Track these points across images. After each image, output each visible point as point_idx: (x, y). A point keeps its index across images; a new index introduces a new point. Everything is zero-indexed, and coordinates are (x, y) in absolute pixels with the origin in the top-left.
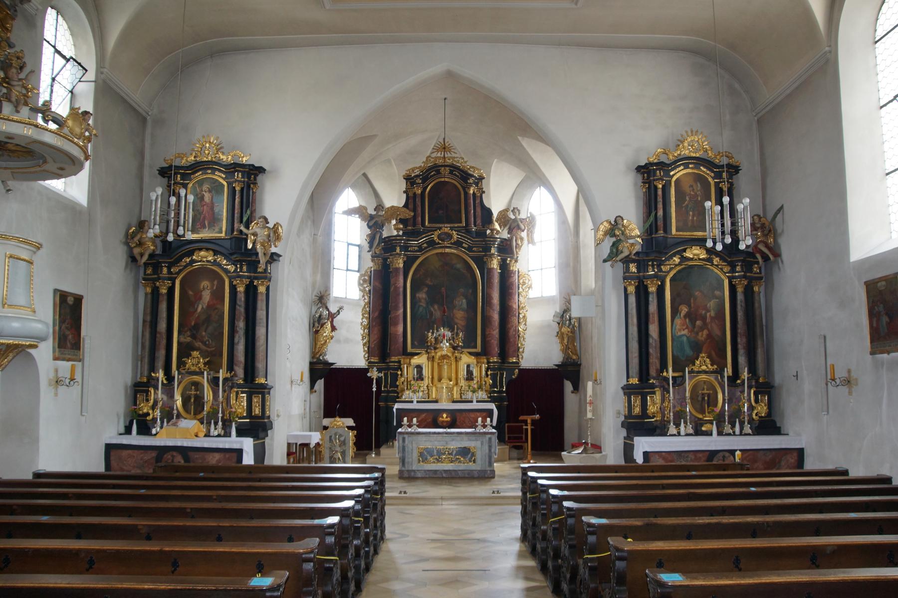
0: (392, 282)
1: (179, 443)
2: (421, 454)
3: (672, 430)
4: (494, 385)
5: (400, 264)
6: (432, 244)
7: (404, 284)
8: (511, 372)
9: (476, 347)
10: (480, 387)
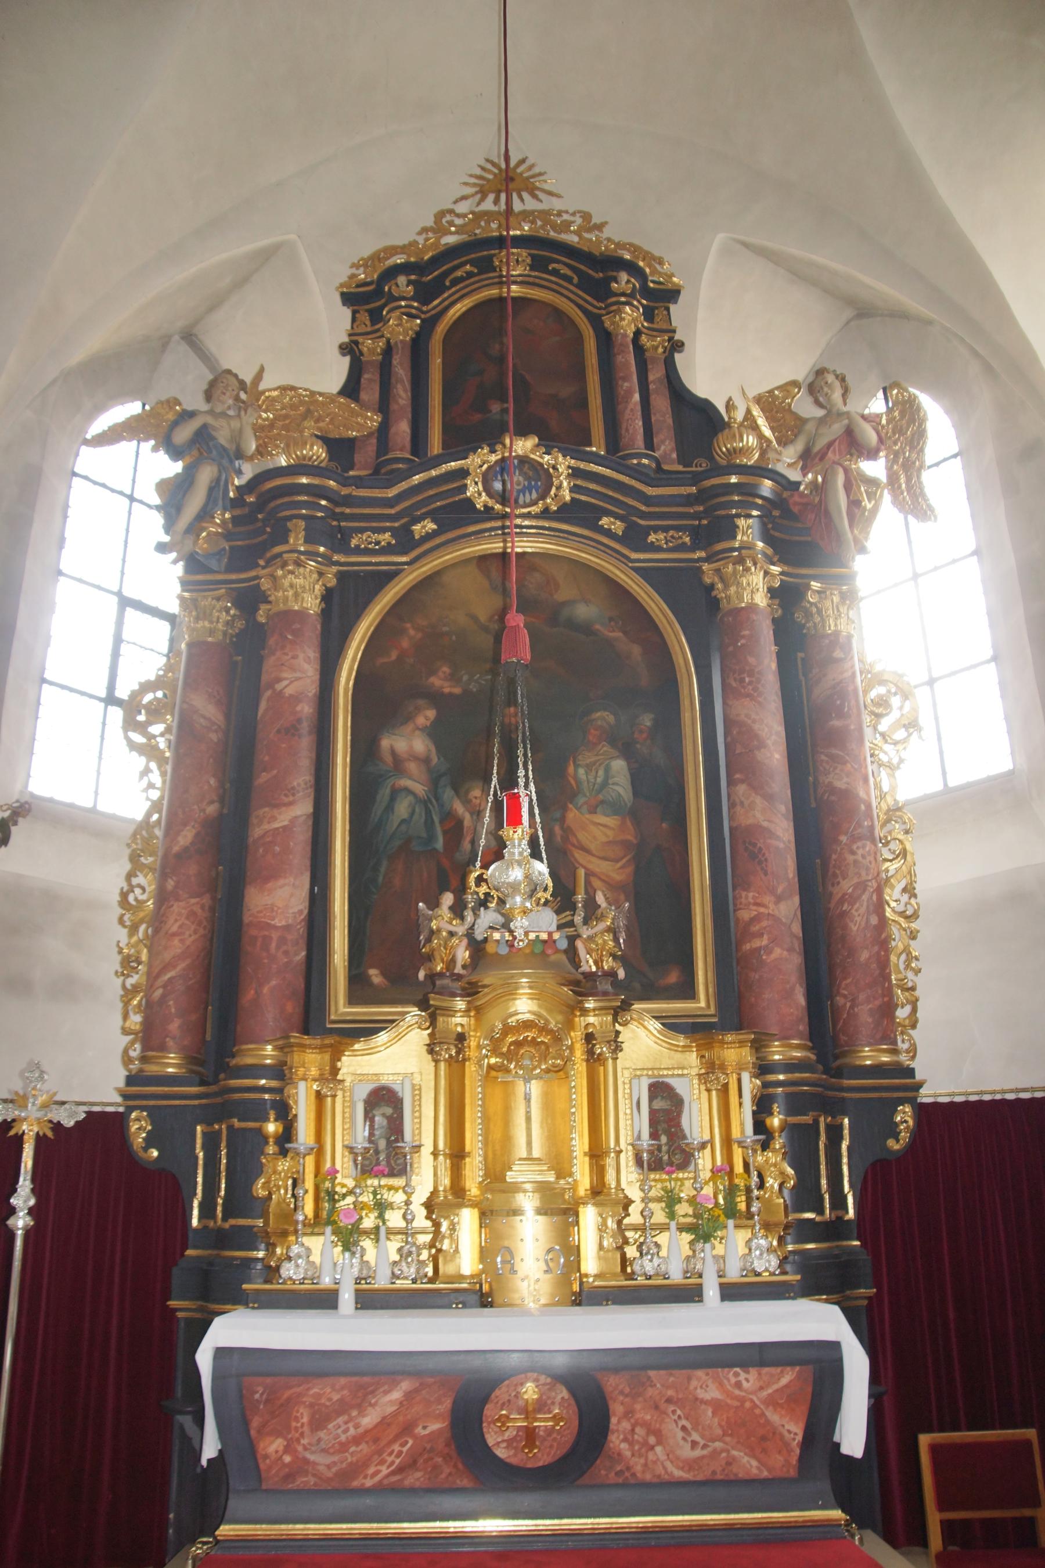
0: (265, 678)
5: (301, 586)
6: (458, 515)
8: (876, 1118)
9: (687, 991)
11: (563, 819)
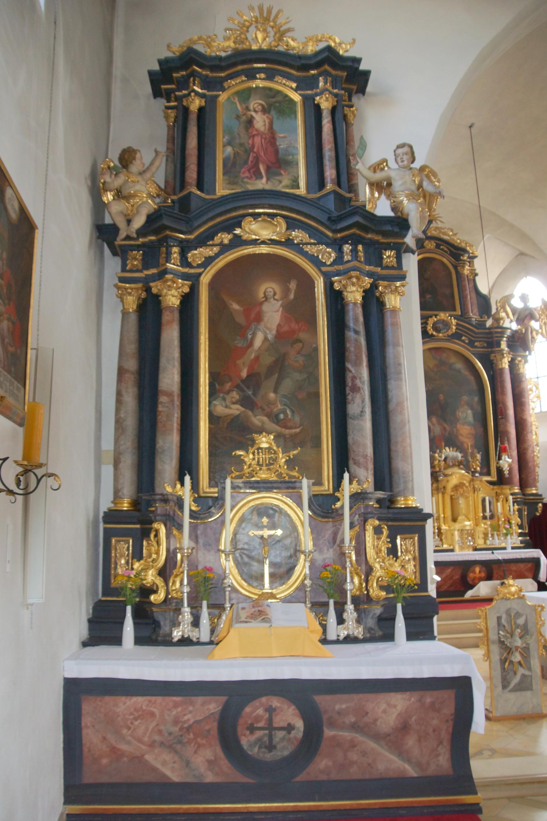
11: (456, 427)
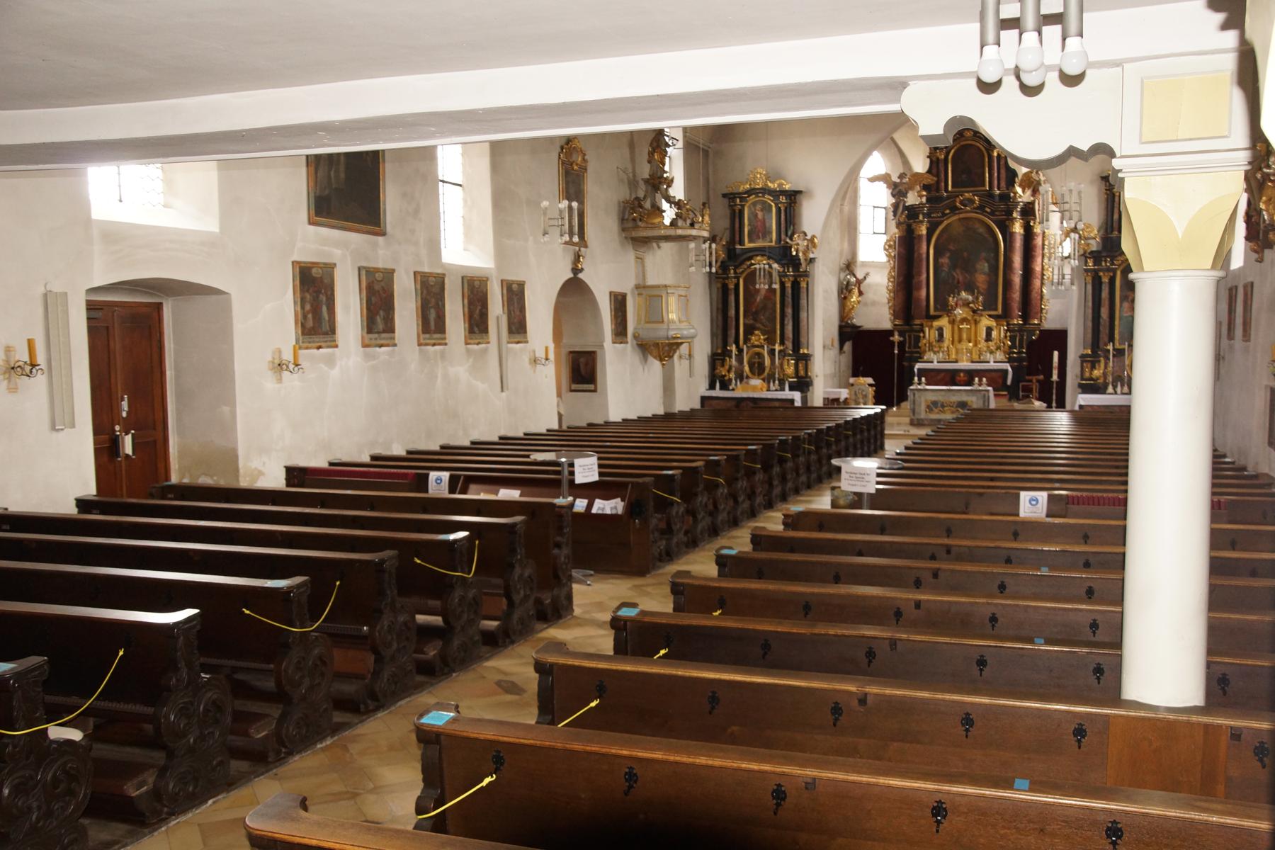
1: (752, 395)
2: (928, 407)
3: (1110, 389)
4: (1010, 347)
6: (954, 209)
7: (927, 251)
9: (996, 309)
10: (998, 348)
